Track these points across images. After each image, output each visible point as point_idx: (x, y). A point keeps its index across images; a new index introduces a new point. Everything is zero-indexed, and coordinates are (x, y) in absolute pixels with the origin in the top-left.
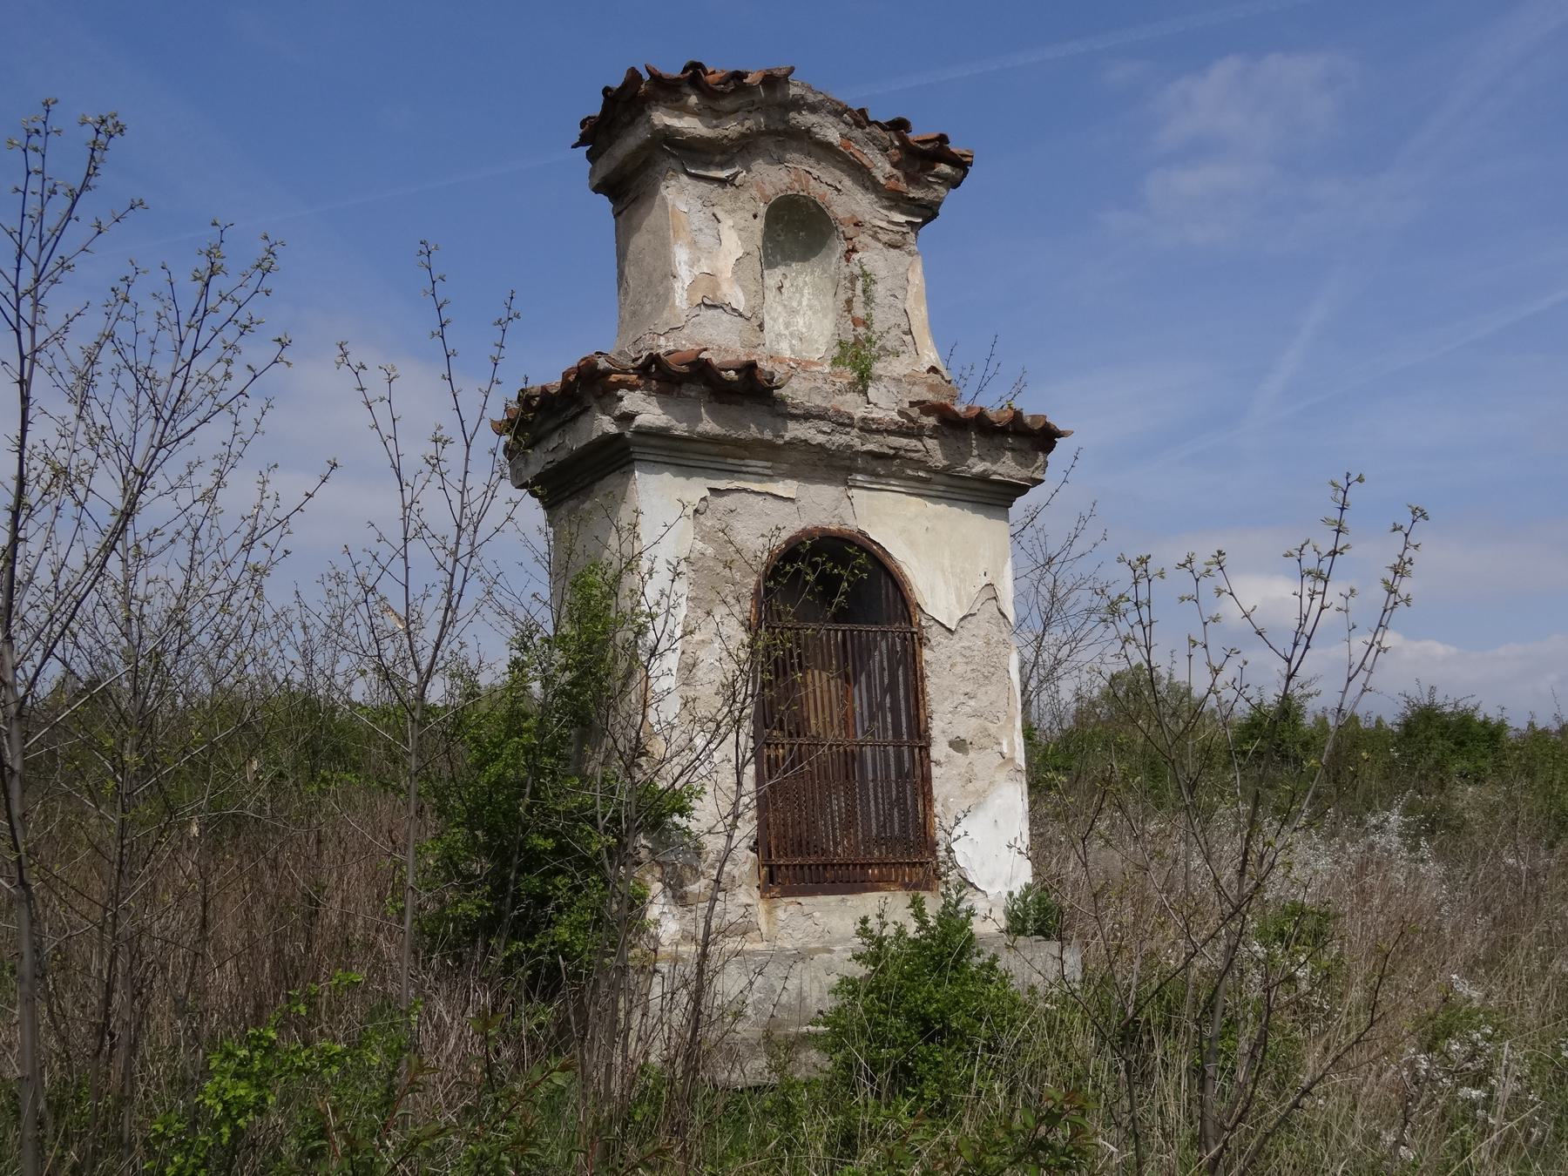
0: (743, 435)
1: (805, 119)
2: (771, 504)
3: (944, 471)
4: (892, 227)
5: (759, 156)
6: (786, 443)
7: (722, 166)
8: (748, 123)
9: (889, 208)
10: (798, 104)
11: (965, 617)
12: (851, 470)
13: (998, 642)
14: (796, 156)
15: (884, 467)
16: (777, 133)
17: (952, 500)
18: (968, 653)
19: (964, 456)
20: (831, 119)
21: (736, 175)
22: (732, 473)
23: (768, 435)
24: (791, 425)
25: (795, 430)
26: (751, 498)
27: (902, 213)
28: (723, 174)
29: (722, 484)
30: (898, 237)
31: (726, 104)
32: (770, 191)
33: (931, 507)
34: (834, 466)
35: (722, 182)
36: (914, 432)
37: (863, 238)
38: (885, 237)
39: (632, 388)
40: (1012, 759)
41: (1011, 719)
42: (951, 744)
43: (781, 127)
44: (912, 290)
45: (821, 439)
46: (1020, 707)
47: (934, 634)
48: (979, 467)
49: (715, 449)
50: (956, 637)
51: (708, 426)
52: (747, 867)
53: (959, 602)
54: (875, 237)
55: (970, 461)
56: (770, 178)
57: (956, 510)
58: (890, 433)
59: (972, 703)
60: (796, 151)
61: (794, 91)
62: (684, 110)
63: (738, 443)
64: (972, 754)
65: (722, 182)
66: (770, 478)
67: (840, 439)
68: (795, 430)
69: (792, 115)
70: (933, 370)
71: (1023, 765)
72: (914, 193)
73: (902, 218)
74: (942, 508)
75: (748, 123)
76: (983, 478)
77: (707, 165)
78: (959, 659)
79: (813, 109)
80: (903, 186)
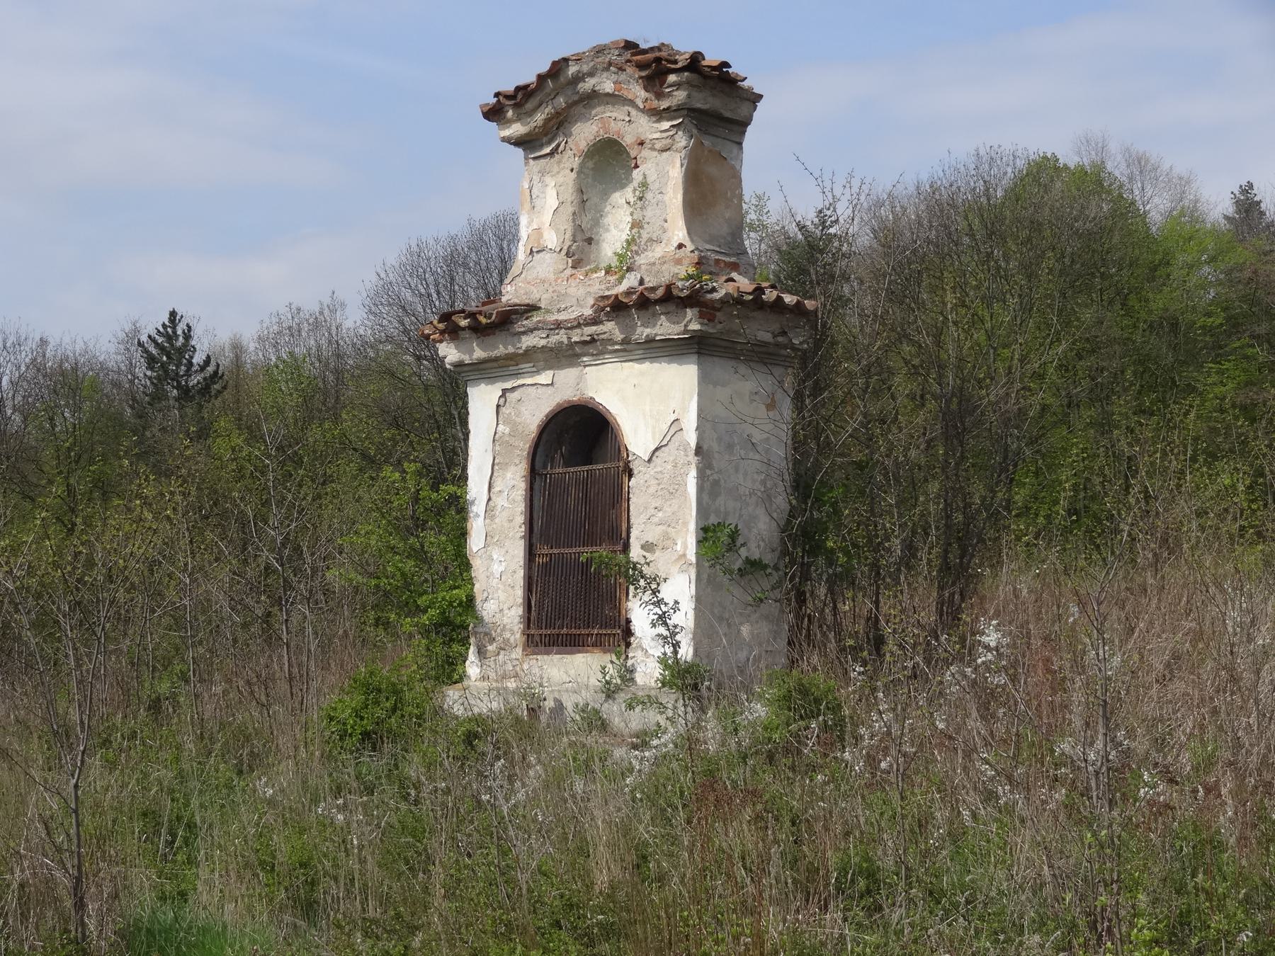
0: (495, 353)
1: (587, 85)
2: (541, 390)
3: (625, 342)
4: (665, 135)
5: (576, 121)
6: (527, 351)
7: (549, 143)
8: (547, 111)
9: (658, 121)
10: (579, 78)
11: (657, 449)
12: (579, 356)
13: (683, 464)
14: (598, 109)
15: (593, 348)
16: (575, 103)
17: (653, 359)
18: (659, 476)
19: (634, 327)
20: (605, 74)
21: (558, 145)
22: (517, 375)
23: (511, 349)
24: (524, 338)
25: (528, 341)
26: (530, 389)
27: (668, 120)
28: (547, 150)
29: (508, 385)
30: (669, 141)
31: (529, 106)
32: (583, 145)
33: (636, 366)
34: (565, 356)
35: (551, 154)
36: (595, 321)
37: (646, 153)
38: (658, 146)
39: (441, 341)
40: (684, 555)
41: (685, 524)
42: (643, 547)
43: (576, 98)
44: (671, 184)
45: (543, 342)
46: (694, 513)
47: (635, 466)
48: (647, 331)
49: (495, 364)
50: (652, 465)
51: (479, 354)
52: (518, 636)
53: (654, 438)
54: (653, 149)
55: (639, 330)
56: (584, 133)
57: (656, 365)
58: (587, 325)
59: (660, 514)
60: (599, 105)
61: (572, 69)
62: (510, 122)
63: (496, 359)
64: (658, 553)
65: (551, 154)
66: (538, 372)
67: (554, 339)
68: (528, 341)
69: (580, 85)
70: (680, 246)
71: (694, 560)
72: (664, 104)
73: (666, 125)
74: (646, 366)
75: (547, 111)
76: (650, 341)
77: (541, 146)
78: (654, 482)
79: (591, 74)
80: (655, 104)
